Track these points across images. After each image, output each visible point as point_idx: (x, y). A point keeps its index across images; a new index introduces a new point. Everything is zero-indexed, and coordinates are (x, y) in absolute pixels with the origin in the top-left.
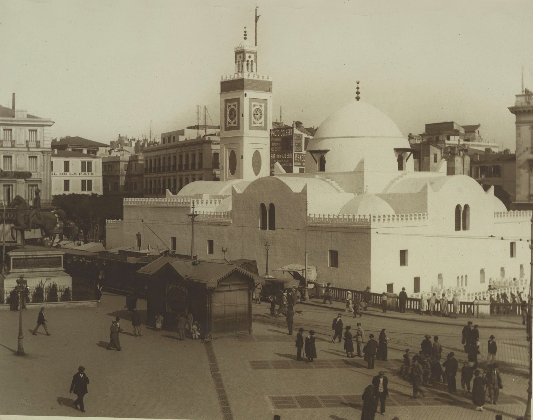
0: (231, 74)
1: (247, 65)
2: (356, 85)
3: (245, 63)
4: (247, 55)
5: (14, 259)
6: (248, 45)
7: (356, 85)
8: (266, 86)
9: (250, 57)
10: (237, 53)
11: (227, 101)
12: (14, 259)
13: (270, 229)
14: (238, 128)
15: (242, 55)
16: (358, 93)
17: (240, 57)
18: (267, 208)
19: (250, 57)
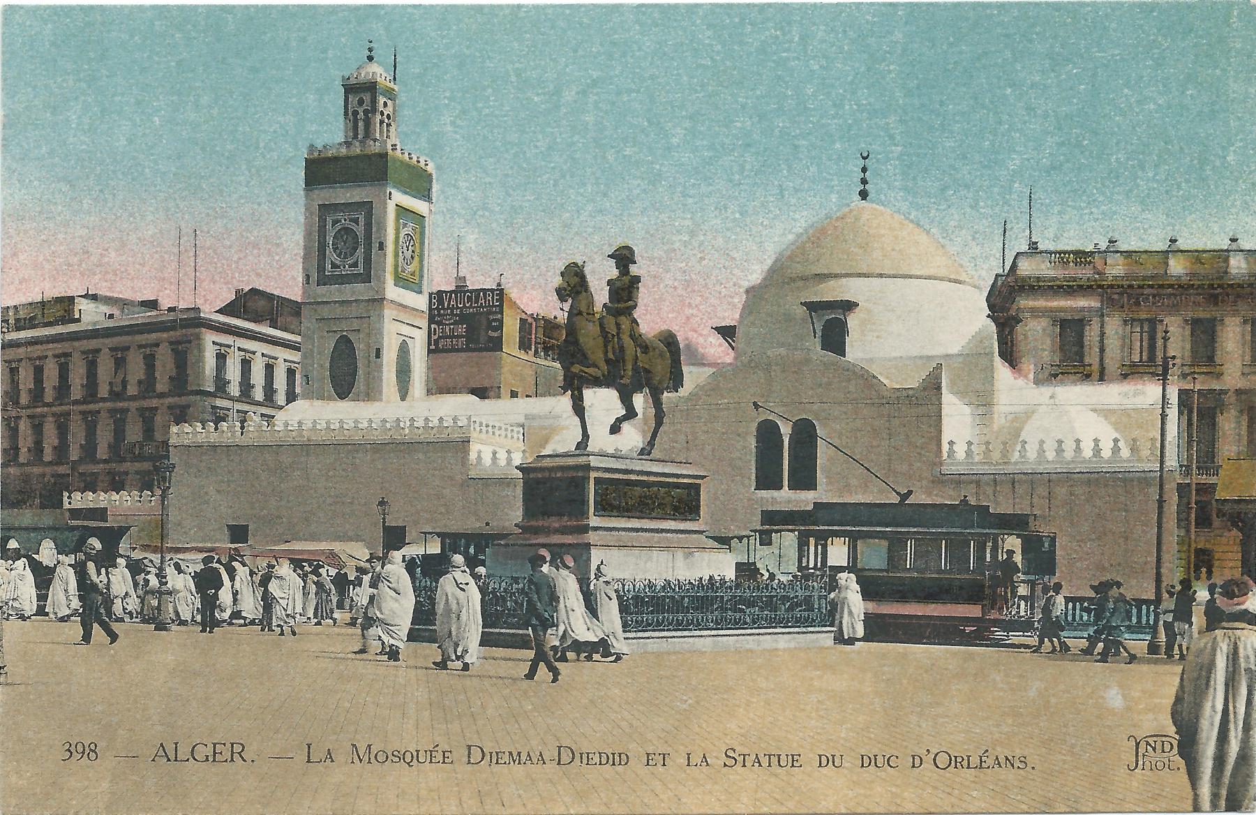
1: (382, 122)
2: (861, 163)
4: (381, 100)
5: (598, 481)
7: (861, 163)
11: (325, 209)
12: (598, 481)
14: (366, 278)
15: (367, 97)
17: (361, 102)
18: (786, 430)
19: (385, 104)
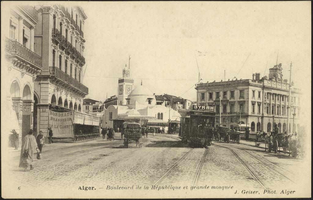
0: (121, 77)
3: (125, 74)
4: (126, 72)
6: (126, 69)
8: (132, 81)
9: (127, 72)
10: (123, 71)
13: (161, 119)
16: (142, 83)
18: (160, 114)
19: (127, 72)
